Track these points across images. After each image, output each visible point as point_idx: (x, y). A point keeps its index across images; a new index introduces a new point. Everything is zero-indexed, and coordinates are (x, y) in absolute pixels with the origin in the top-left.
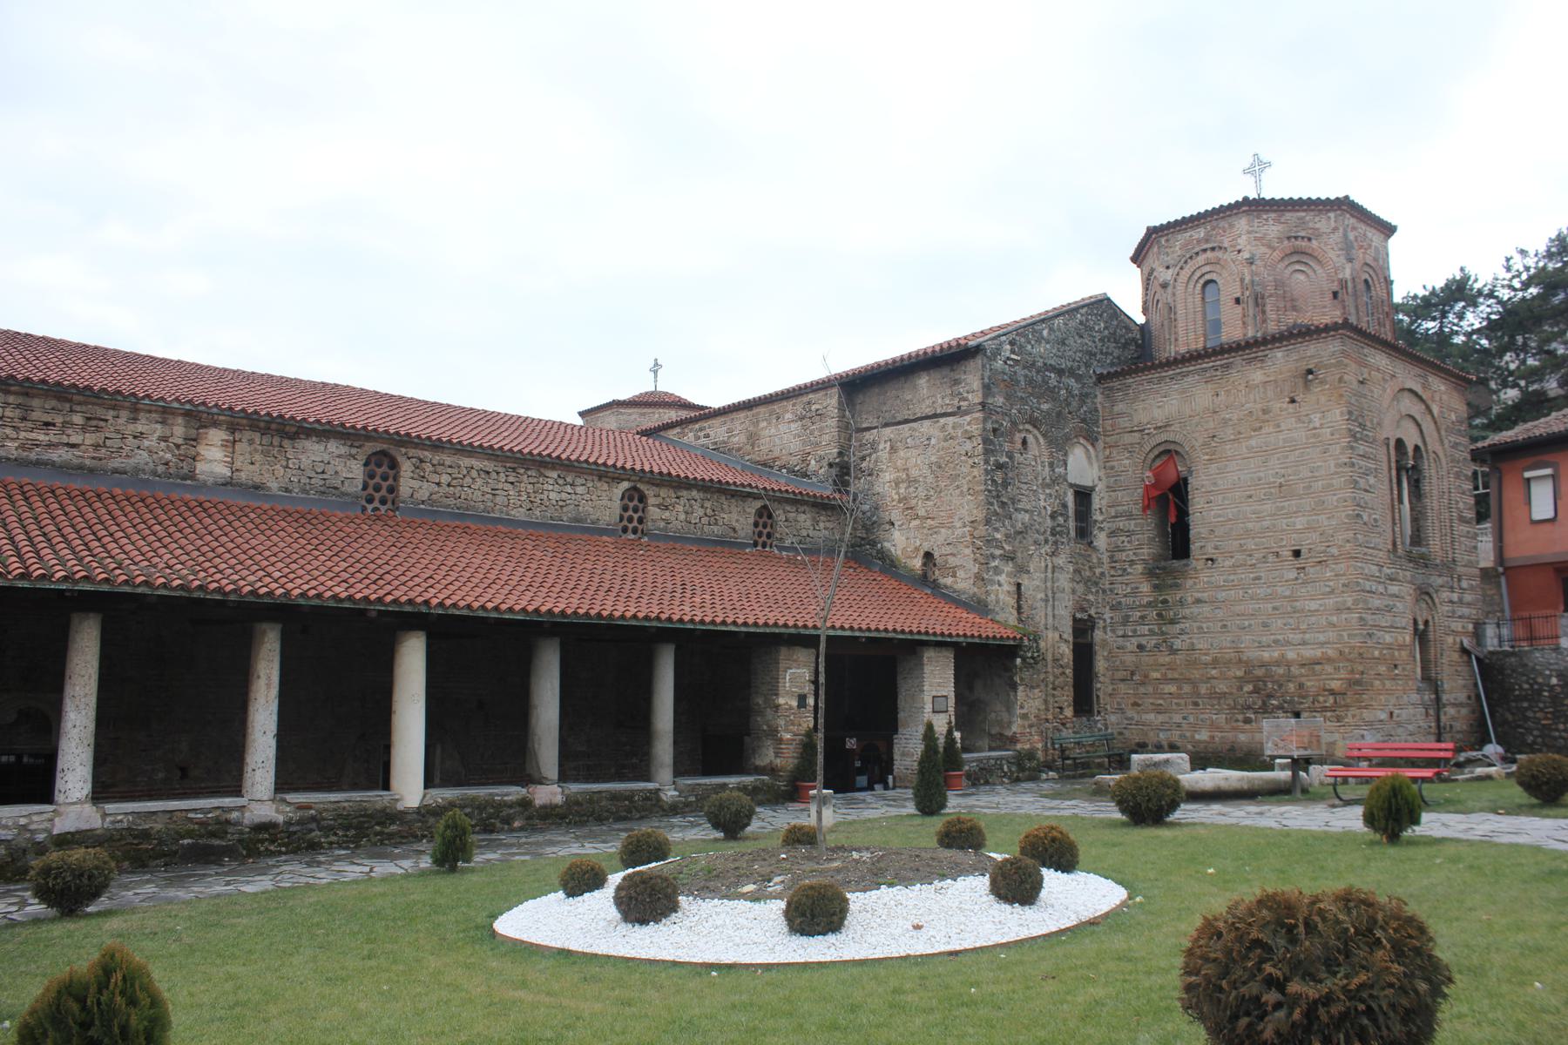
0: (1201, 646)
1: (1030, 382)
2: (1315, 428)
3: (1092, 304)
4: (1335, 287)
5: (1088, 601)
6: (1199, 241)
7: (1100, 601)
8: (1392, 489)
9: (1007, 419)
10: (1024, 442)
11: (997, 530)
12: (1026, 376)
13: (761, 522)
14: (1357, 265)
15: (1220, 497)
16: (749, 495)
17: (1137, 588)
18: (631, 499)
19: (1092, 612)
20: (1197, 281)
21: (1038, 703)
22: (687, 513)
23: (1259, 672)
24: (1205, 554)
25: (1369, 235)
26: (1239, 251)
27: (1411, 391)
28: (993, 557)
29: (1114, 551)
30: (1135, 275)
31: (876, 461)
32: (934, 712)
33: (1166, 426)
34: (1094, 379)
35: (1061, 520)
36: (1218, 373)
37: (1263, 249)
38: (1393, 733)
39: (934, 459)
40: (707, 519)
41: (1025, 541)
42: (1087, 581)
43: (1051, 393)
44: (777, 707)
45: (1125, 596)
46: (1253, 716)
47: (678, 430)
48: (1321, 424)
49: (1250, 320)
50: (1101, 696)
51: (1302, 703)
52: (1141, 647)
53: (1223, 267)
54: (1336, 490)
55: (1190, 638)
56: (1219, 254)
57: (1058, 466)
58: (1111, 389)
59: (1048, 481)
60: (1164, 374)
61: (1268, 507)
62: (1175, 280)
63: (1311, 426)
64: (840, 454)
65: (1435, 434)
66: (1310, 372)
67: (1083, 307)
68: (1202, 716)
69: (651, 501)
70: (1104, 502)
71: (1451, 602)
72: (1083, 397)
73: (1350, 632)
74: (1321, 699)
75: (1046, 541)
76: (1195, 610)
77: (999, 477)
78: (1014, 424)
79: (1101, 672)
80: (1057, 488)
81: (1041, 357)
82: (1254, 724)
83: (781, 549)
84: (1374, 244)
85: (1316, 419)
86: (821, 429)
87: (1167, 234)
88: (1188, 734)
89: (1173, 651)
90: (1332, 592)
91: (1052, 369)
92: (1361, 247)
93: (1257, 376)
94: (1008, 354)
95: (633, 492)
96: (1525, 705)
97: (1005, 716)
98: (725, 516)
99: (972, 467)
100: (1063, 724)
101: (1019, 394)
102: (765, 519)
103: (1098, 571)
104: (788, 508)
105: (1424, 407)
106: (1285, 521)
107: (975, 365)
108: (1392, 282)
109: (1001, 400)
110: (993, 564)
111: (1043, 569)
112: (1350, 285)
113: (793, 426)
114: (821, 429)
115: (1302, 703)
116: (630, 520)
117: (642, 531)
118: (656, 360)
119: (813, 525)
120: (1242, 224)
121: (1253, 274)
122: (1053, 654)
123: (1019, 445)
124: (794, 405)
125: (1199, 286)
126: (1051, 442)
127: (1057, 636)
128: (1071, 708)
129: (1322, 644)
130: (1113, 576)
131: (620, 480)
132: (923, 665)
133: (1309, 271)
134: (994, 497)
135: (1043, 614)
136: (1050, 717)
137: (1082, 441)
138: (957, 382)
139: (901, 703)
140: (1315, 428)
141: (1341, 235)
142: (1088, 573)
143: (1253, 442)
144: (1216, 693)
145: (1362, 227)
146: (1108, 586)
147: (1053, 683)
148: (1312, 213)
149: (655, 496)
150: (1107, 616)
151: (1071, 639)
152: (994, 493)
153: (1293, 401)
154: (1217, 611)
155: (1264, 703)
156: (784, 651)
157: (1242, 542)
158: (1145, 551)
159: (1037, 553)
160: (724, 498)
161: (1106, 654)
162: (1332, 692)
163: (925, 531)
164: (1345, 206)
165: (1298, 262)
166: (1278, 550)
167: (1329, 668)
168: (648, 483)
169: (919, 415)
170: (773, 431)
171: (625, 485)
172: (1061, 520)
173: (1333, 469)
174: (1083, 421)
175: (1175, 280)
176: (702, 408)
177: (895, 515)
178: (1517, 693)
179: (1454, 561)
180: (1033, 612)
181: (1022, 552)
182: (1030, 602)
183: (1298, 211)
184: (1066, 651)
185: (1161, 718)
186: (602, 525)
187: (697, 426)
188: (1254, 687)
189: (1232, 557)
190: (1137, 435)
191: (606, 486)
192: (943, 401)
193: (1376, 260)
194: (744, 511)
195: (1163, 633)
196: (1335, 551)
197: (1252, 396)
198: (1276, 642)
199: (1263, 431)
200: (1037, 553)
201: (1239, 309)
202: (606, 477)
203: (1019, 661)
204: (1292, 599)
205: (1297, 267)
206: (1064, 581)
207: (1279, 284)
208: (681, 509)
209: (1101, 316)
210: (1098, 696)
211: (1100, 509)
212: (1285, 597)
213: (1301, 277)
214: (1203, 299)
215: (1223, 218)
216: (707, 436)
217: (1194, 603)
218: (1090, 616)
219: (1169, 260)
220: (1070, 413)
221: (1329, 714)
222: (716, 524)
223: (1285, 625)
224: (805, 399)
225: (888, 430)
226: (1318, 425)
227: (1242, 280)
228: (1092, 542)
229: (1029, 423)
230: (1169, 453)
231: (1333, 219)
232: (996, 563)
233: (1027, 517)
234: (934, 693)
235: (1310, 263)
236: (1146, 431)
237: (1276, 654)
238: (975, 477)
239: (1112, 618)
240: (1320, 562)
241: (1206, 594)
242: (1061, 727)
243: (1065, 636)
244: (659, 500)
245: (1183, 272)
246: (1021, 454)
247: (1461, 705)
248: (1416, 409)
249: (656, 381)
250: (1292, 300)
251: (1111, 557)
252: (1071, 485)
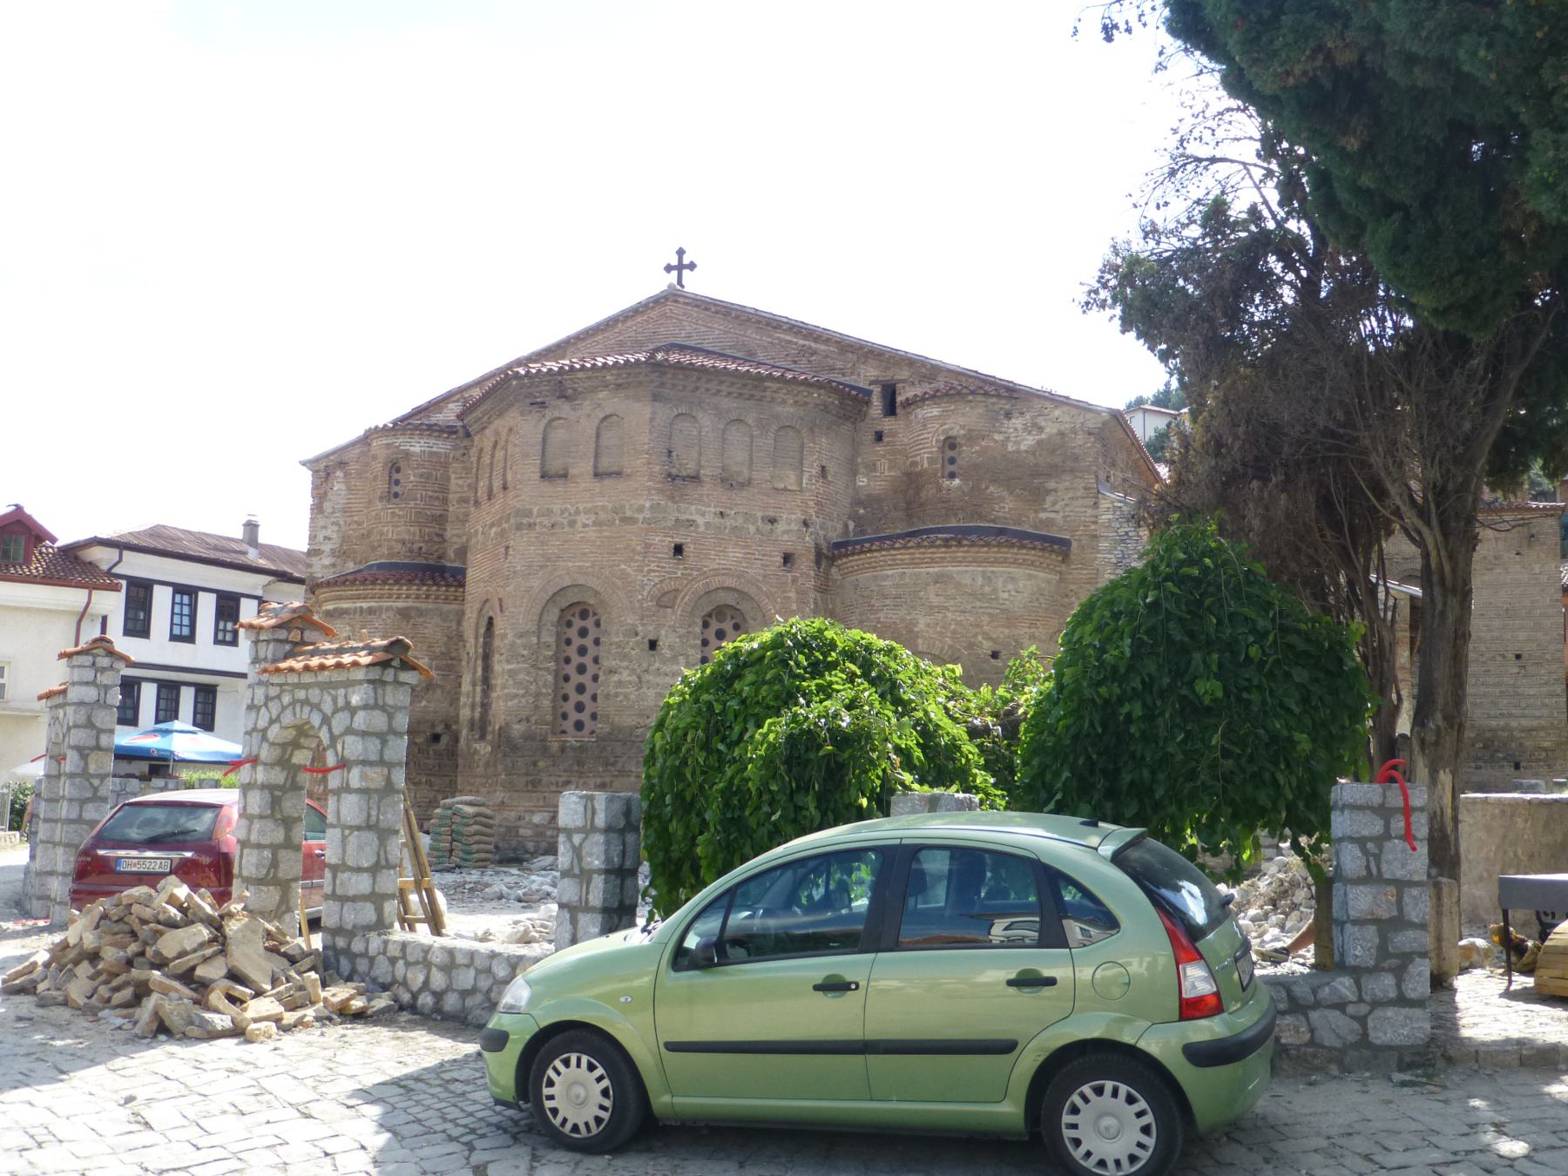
23: (1488, 735)
61: (1497, 623)
90: (1546, 683)
129: (1539, 717)
143: (1486, 578)
155: (1492, 756)
162: (1544, 749)
167: (1542, 734)
173: (1548, 602)
196: (1548, 656)
198: (1502, 715)
204: (1514, 686)
237: (1502, 723)
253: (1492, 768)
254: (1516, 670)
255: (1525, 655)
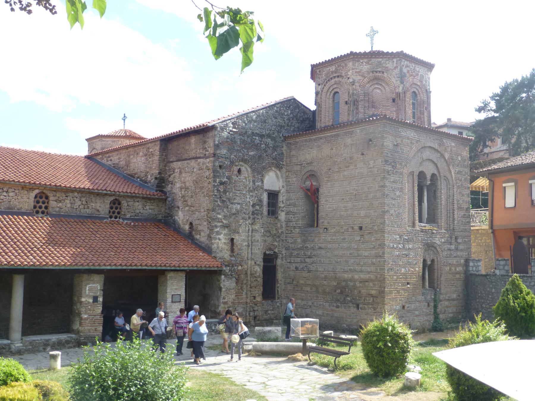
0: (320, 270)
1: (243, 141)
2: (371, 168)
3: (284, 102)
4: (394, 96)
5: (274, 245)
6: (332, 72)
7: (280, 245)
8: (414, 196)
9: (228, 160)
10: (239, 171)
11: (219, 214)
12: (241, 139)
13: (114, 206)
14: (408, 85)
15: (331, 199)
16: (106, 194)
17: (296, 240)
18: (41, 198)
19: (276, 250)
20: (331, 92)
21: (233, 296)
22: (71, 203)
23: (343, 284)
24: (323, 226)
25: (417, 69)
26: (348, 78)
27: (430, 147)
28: (216, 227)
29: (288, 221)
30: (311, 86)
31: (174, 178)
32: (172, 302)
33: (311, 163)
34: (282, 139)
35: (258, 207)
36: (333, 139)
37: (359, 78)
38: (404, 315)
39: (195, 178)
40: (83, 206)
41: (237, 218)
42: (273, 236)
43: (256, 147)
44: (81, 302)
45: (291, 243)
46: (340, 305)
47: (100, 156)
48: (373, 166)
49: (351, 113)
50: (279, 290)
51: (360, 300)
52: (297, 268)
53: (341, 86)
54: (378, 198)
55: (316, 265)
56: (340, 79)
57: (257, 182)
58: (290, 144)
59: (251, 189)
60: (312, 138)
61: (350, 205)
62: (322, 91)
63: (369, 167)
64: (160, 173)
65: (446, 168)
66: (370, 140)
67: (278, 103)
68: (319, 303)
69: (51, 198)
70: (284, 198)
71: (450, 250)
72: (275, 148)
73: (381, 267)
74: (367, 299)
75: (249, 218)
76: (319, 252)
77: (221, 188)
78: (232, 163)
79: (280, 279)
80: (257, 192)
81: (251, 129)
82: (340, 308)
83: (124, 219)
84: (420, 73)
85: (371, 162)
86: (153, 161)
87: (319, 68)
88: (314, 311)
89: (309, 271)
90: (374, 248)
91: (257, 135)
92: (411, 75)
93: (349, 141)
94: (231, 129)
95: (42, 194)
96: (483, 301)
97: (216, 302)
98: (93, 205)
99: (209, 183)
100: (256, 305)
101: (236, 148)
102: (117, 205)
103: (280, 231)
104: (129, 200)
105: (439, 155)
106: (356, 212)
107: (211, 134)
108: (430, 92)
109: (225, 151)
110: (216, 230)
111: (247, 231)
112: (401, 95)
113: (143, 158)
114: (153, 161)
115: (360, 300)
116: (40, 207)
117: (47, 212)
118: (124, 114)
119: (143, 208)
120: (350, 64)
121: (353, 89)
122: (251, 271)
123: (236, 172)
124: (143, 148)
125: (332, 94)
126: (254, 170)
127: (253, 263)
128: (261, 297)
130: (287, 233)
131: (32, 189)
132: (167, 280)
133: (382, 88)
134: (218, 198)
135: (246, 252)
136: (248, 301)
137: (273, 169)
138: (205, 142)
139: (159, 297)
140: (371, 168)
141: (399, 70)
142: (275, 232)
143: (346, 173)
144: (326, 292)
145: (412, 66)
146: (285, 238)
147: (250, 285)
148: (385, 59)
149: (54, 196)
150: (284, 252)
151: (262, 264)
152: (218, 196)
153: (363, 154)
154: (328, 253)
155: (345, 299)
156: (85, 276)
157: (339, 221)
158: (300, 222)
159: (244, 223)
160: (93, 196)
161: (282, 270)
162: (372, 296)
163: (190, 212)
164: (401, 56)
165: (377, 84)
166: (353, 226)
167: (371, 284)
168: (49, 190)
169: (191, 157)
170: (135, 160)
171: (37, 191)
172: (258, 207)
173: (377, 188)
174: (275, 159)
175: (322, 91)
176: (140, 138)
177: (180, 204)
178: (479, 295)
179: (454, 229)
180: (241, 251)
181: (235, 223)
182: (239, 247)
183: (378, 58)
184: (259, 270)
185: (304, 303)
186: (23, 210)
187: (107, 155)
188: (341, 290)
189: (334, 228)
190: (299, 166)
191: (26, 192)
192: (199, 152)
193: (421, 81)
194: (104, 202)
195: (305, 262)
196: (376, 228)
197: (346, 151)
198: (350, 270)
199: (350, 168)
200: (244, 223)
201: (346, 107)
202: (26, 188)
203: (223, 277)
204: (357, 250)
205: (376, 86)
206: (258, 236)
207: (366, 94)
208: (68, 202)
209: (289, 107)
210: (278, 291)
211: (282, 201)
212: (355, 249)
213: (379, 91)
214: (333, 101)
215: (342, 61)
216: (111, 160)
217: (318, 249)
218: (274, 252)
219: (320, 81)
220: (267, 156)
221: (370, 306)
222: (88, 208)
223: (354, 262)
224: (147, 146)
225: (179, 163)
226: (372, 166)
227: (349, 93)
228: (278, 217)
229: (242, 161)
230: (312, 175)
231: (395, 62)
232: (218, 229)
233: (239, 207)
234: (173, 293)
235: (383, 85)
236: (303, 165)
237: (350, 276)
238: (209, 188)
239: (286, 253)
240: (370, 233)
241: (323, 245)
242: (254, 305)
243: (258, 263)
244: (56, 198)
245: (325, 88)
246: (237, 176)
247: (453, 300)
248: (434, 156)
249: (124, 125)
250: (373, 102)
251: (286, 224)
252: (266, 190)
253: (345, 307)
254: (358, 238)
255: (364, 227)
